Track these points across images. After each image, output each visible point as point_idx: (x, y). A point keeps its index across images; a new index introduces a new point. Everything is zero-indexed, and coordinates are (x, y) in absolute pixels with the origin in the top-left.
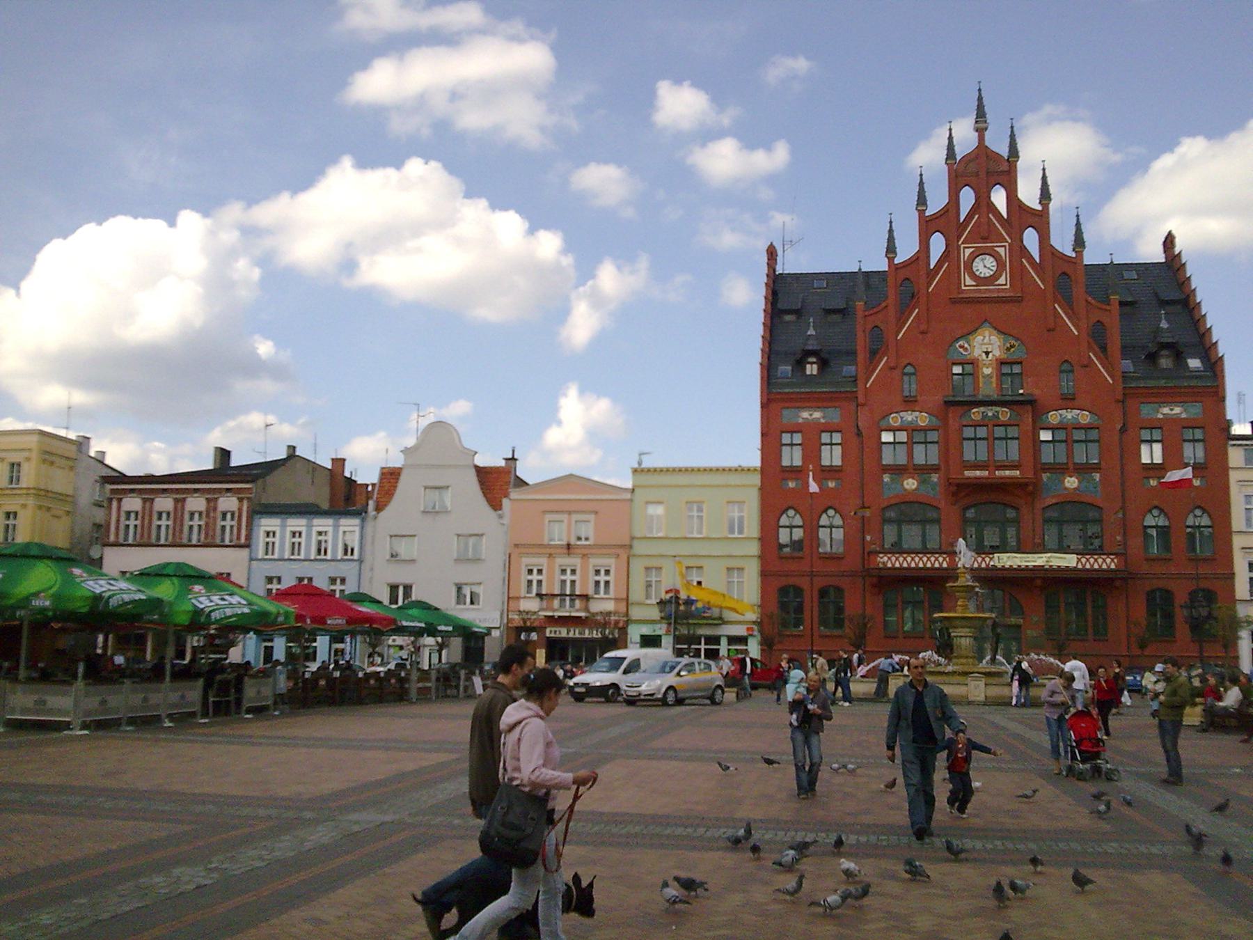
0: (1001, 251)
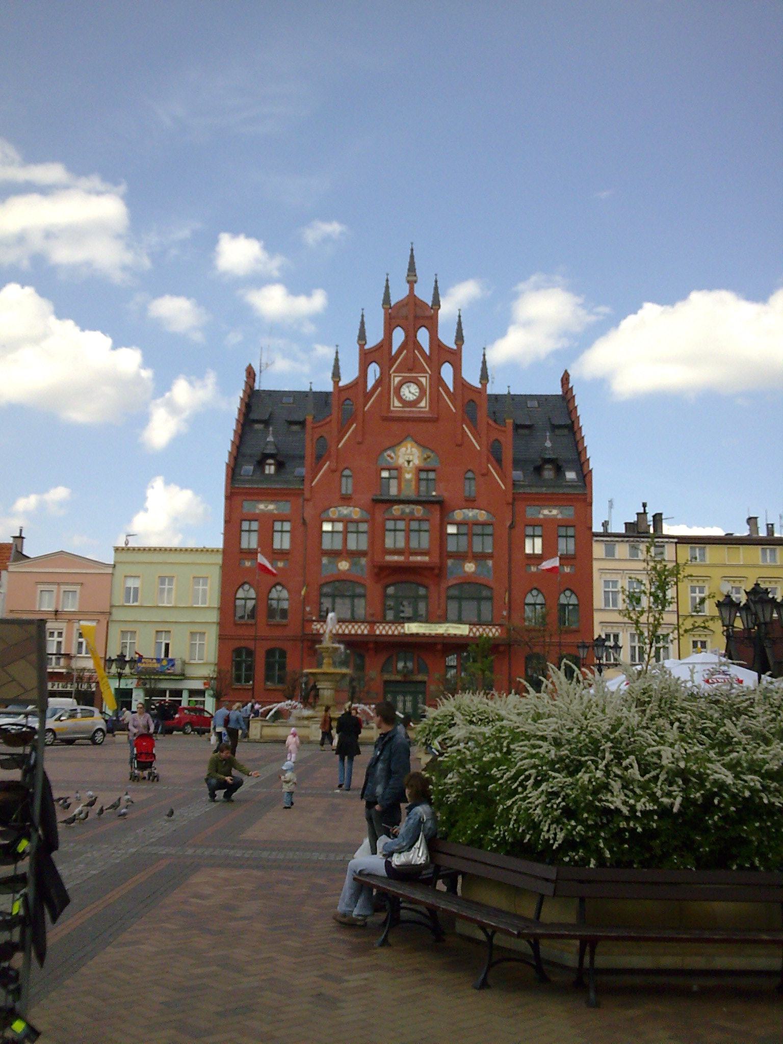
0: (423, 380)
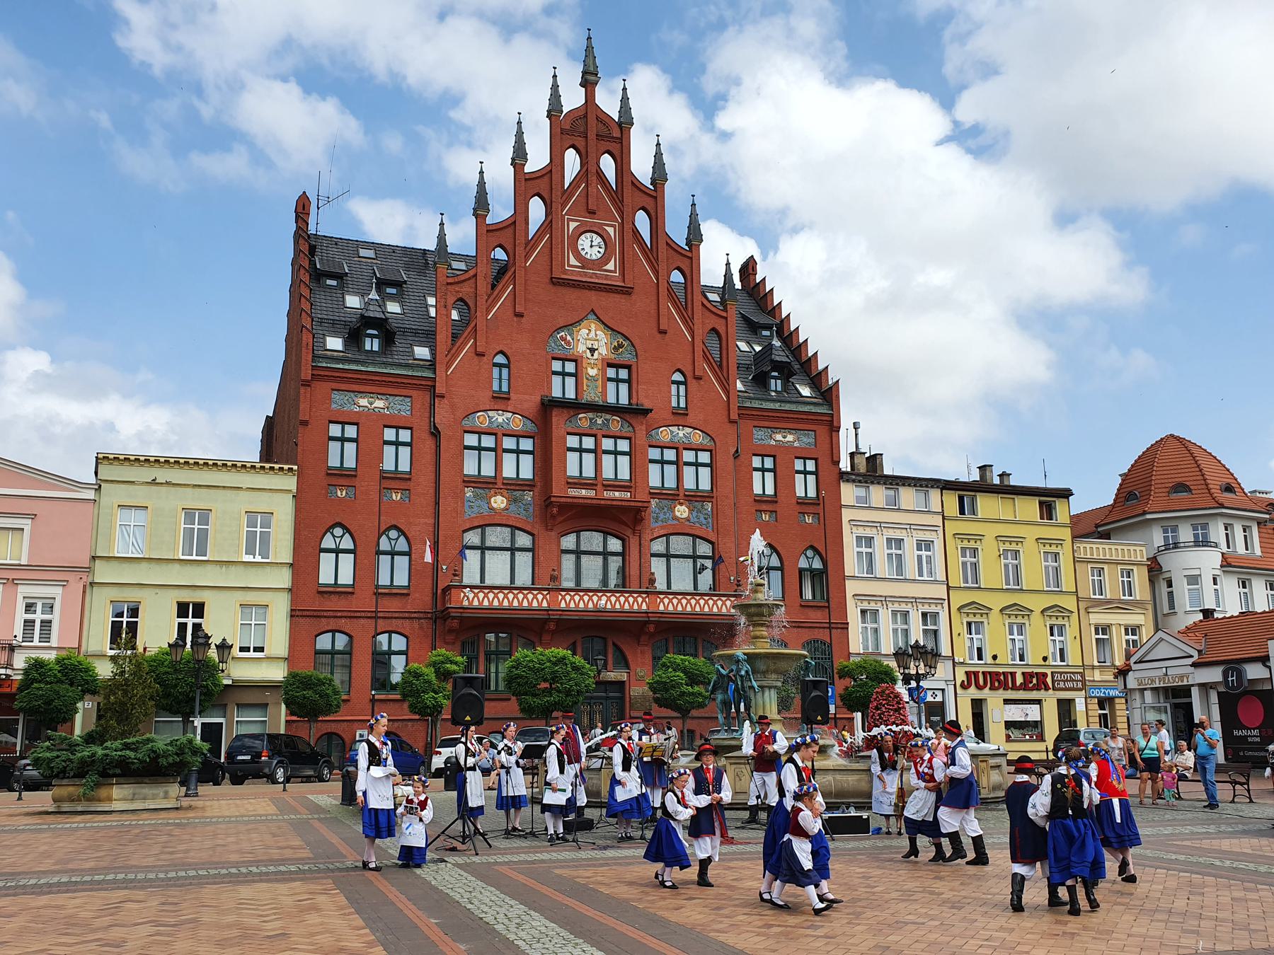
0: (611, 230)
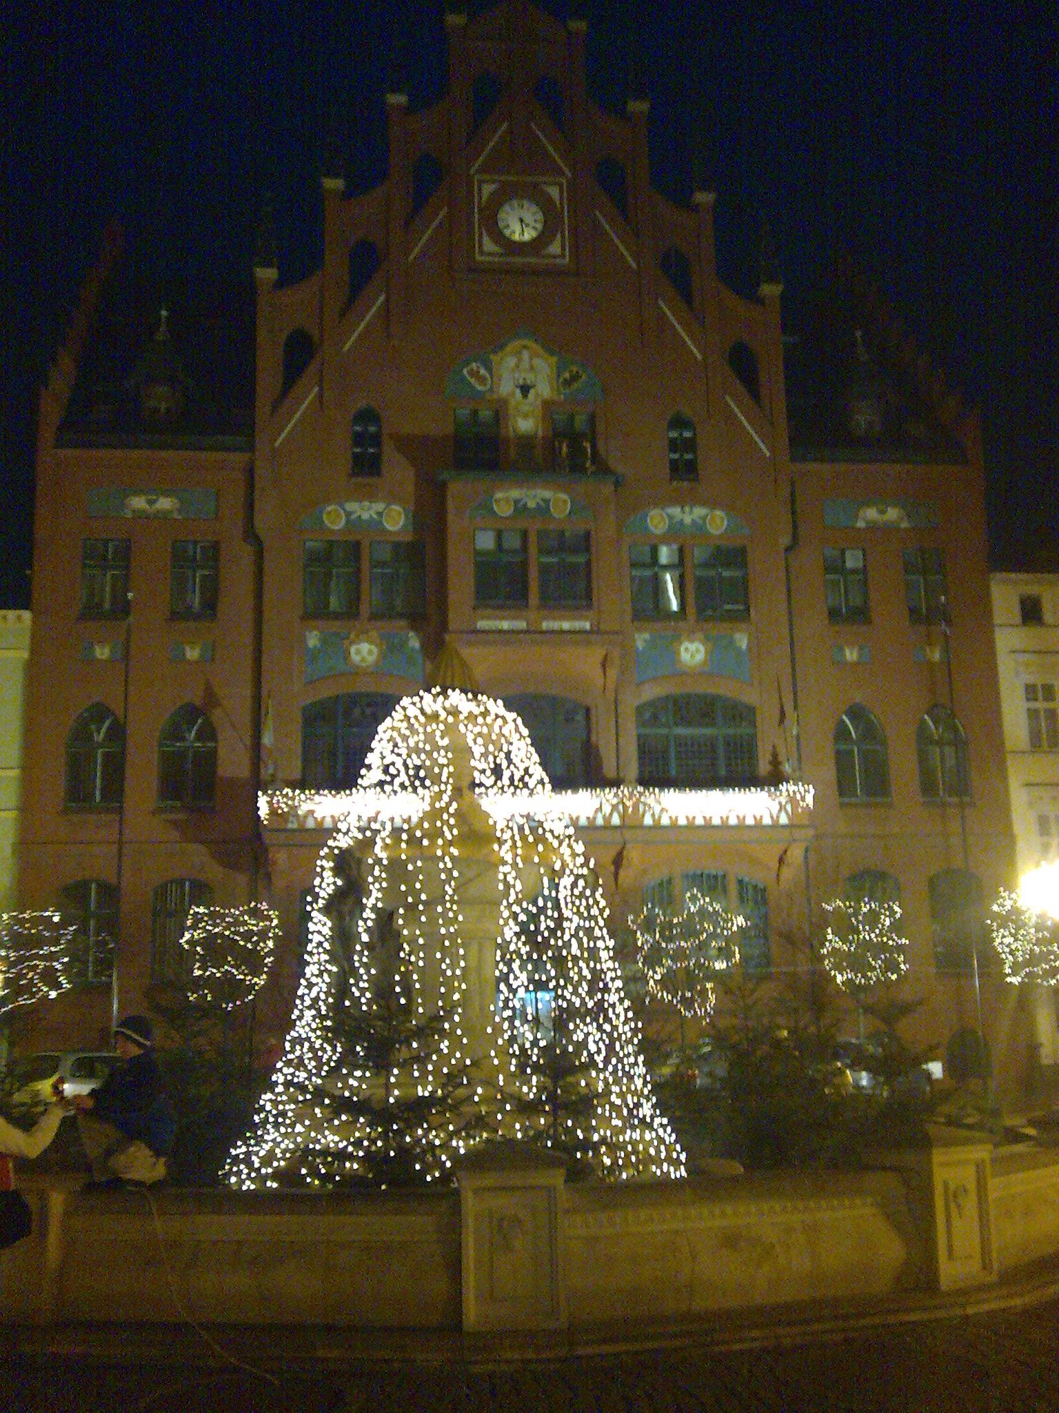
0: (554, 192)
